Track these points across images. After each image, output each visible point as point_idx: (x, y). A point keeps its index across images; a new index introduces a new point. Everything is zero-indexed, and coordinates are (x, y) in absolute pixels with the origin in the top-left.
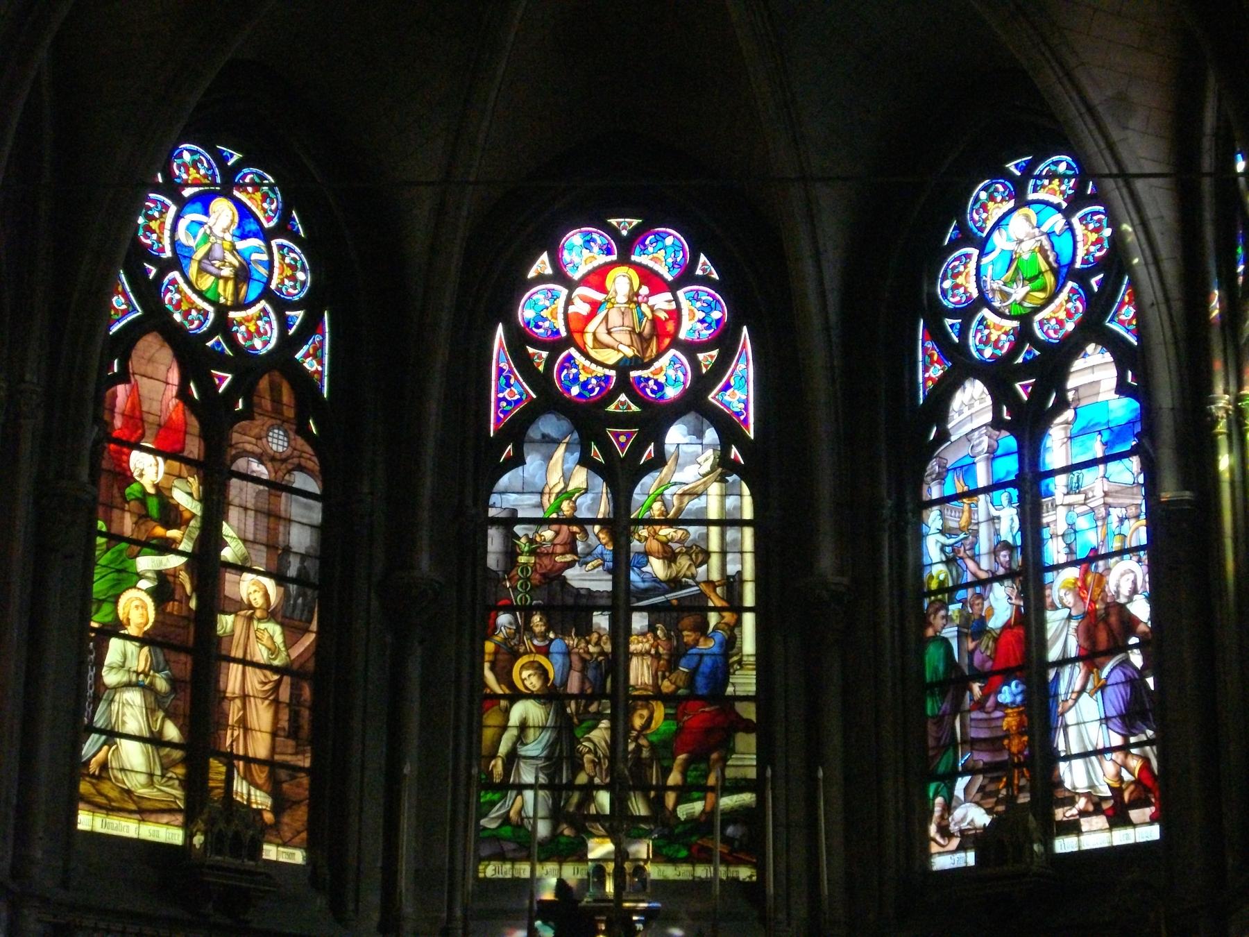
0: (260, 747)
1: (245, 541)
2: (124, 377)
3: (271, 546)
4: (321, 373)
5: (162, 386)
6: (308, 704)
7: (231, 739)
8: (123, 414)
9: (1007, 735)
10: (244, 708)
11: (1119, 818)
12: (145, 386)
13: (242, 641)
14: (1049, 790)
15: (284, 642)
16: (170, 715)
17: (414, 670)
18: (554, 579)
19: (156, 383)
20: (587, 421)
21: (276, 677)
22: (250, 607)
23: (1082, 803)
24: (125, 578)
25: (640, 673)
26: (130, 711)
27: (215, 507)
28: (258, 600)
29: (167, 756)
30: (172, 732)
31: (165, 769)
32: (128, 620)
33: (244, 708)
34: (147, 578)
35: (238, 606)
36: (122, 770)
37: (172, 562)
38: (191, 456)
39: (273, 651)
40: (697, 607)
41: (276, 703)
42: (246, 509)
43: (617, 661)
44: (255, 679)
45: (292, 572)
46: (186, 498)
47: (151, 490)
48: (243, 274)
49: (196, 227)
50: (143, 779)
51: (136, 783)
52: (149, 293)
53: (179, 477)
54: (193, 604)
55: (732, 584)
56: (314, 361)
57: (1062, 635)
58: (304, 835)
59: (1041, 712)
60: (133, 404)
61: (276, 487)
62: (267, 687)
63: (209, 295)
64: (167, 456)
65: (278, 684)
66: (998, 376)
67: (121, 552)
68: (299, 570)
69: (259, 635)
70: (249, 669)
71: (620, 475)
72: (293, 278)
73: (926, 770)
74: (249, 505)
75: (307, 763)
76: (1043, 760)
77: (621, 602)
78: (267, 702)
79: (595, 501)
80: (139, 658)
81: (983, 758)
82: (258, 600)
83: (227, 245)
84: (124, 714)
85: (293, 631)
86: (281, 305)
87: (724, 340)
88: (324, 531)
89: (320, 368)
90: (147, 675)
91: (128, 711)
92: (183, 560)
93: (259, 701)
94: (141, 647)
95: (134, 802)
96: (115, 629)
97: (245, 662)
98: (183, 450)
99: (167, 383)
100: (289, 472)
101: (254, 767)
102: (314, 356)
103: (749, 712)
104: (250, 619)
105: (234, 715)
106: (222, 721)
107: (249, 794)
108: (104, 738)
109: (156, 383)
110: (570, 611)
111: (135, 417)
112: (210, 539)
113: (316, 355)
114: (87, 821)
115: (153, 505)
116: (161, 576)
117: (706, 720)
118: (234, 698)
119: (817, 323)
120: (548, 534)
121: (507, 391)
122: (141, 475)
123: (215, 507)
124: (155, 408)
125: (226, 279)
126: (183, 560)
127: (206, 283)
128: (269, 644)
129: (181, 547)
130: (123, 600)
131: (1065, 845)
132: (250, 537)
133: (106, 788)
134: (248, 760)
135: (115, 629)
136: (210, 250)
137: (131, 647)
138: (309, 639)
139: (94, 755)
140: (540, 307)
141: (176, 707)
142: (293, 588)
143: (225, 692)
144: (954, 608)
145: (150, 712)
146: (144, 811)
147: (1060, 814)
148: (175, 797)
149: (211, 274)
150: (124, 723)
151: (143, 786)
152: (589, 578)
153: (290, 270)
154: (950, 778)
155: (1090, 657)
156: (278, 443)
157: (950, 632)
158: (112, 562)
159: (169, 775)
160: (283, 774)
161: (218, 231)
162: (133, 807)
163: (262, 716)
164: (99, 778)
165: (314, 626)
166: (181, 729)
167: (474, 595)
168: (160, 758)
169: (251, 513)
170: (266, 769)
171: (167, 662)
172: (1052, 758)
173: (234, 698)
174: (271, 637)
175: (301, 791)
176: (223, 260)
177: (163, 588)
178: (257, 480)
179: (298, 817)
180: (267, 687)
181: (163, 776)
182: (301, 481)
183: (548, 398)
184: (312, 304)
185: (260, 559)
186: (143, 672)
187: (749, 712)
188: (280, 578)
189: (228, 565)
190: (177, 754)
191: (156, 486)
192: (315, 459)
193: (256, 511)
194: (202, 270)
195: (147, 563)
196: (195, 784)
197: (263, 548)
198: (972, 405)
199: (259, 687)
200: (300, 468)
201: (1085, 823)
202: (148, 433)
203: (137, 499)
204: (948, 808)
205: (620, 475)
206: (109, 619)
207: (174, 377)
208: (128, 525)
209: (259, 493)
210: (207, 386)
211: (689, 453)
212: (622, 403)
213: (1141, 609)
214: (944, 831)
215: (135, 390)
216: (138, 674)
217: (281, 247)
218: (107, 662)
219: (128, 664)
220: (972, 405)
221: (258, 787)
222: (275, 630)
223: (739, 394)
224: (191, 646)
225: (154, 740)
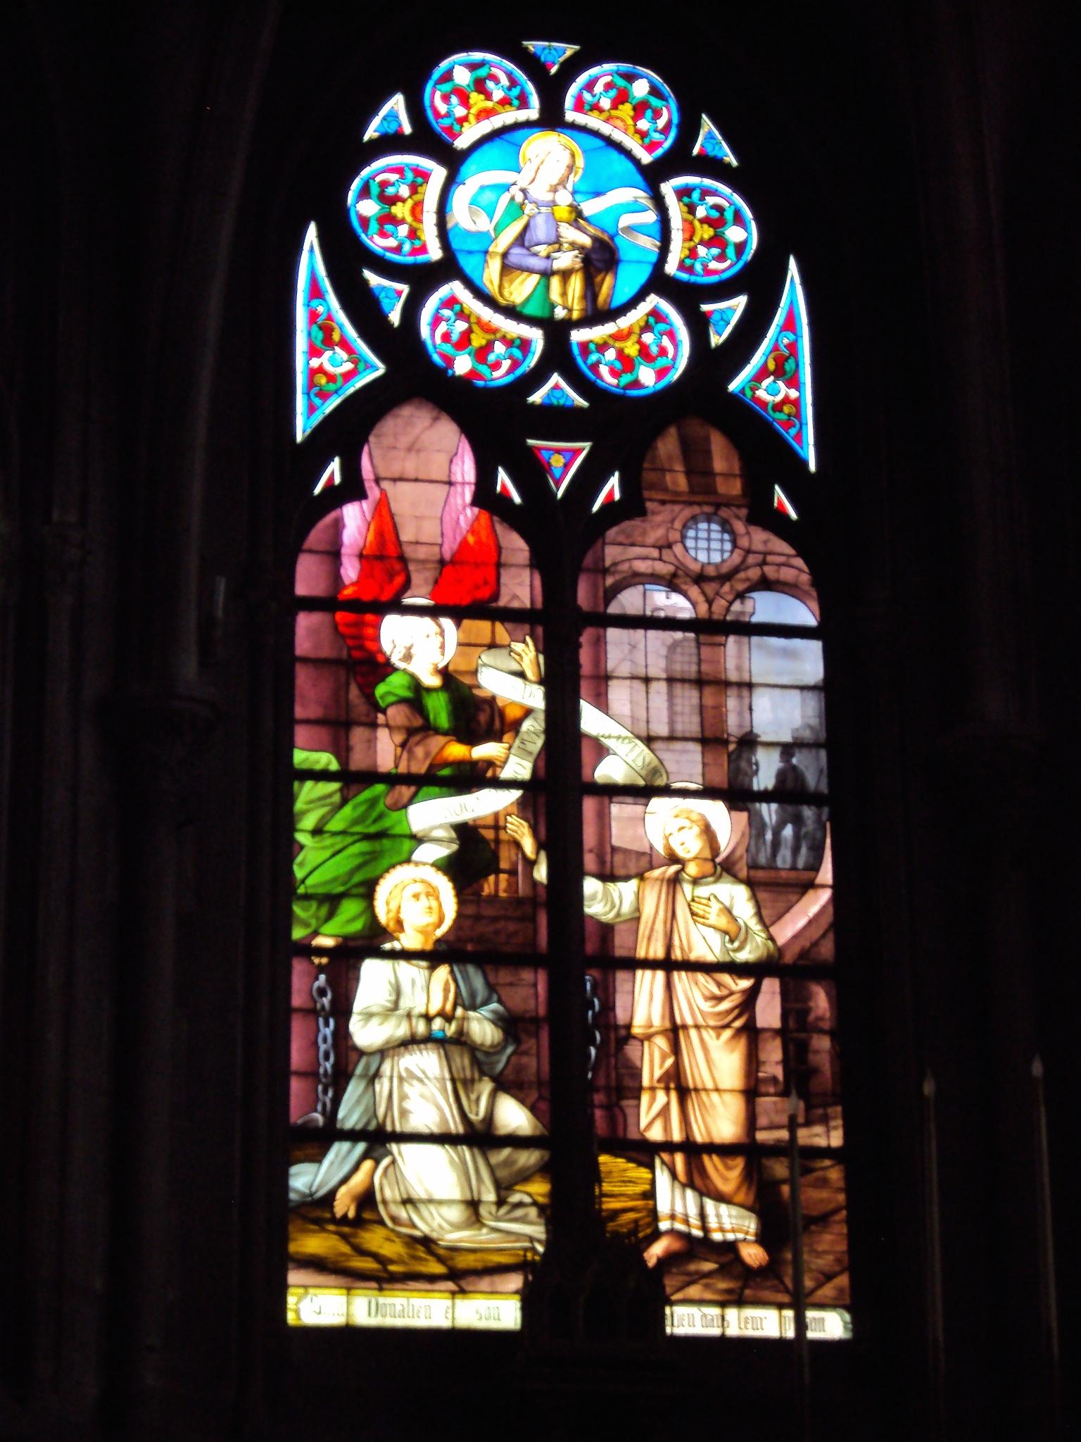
0: (721, 1120)
1: (649, 740)
2: (352, 489)
3: (711, 740)
4: (797, 403)
5: (441, 491)
6: (826, 1025)
7: (653, 1116)
8: (361, 556)
10: (676, 1049)
12: (403, 499)
13: (659, 927)
15: (759, 914)
16: (503, 1085)
21: (745, 984)
22: (673, 859)
24: (382, 845)
26: (421, 1092)
27: (565, 684)
28: (690, 845)
29: (508, 1163)
30: (513, 1116)
31: (503, 1188)
32: (400, 924)
33: (676, 1049)
34: (437, 840)
35: (640, 864)
36: (408, 1201)
37: (481, 805)
38: (516, 604)
39: (734, 934)
41: (751, 1034)
42: (647, 680)
44: (694, 994)
45: (765, 779)
46: (511, 678)
47: (434, 681)
48: (601, 258)
49: (488, 196)
50: (456, 1214)
51: (444, 1224)
53: (492, 645)
54: (541, 873)
56: (783, 381)
58: (843, 1280)
60: (380, 534)
61: (709, 629)
62: (726, 1005)
63: (530, 310)
64: (459, 614)
65: (751, 996)
67: (373, 802)
68: (781, 776)
70: (681, 980)
72: (717, 241)
74: (652, 672)
75: (836, 1139)
78: (728, 1033)
80: (429, 989)
82: (690, 845)
83: (563, 212)
84: (403, 1097)
85: (772, 887)
86: (688, 297)
88: (834, 691)
89: (793, 394)
90: (449, 1018)
91: (412, 1089)
92: (516, 794)
93: (709, 1036)
94: (432, 968)
95: (440, 1260)
96: (372, 941)
97: (668, 965)
98: (496, 596)
99: (450, 483)
100: (741, 596)
101: (712, 1164)
102: (779, 373)
104: (674, 882)
105: (652, 1062)
106: (628, 1082)
107: (703, 1216)
108: (361, 1147)
109: (428, 483)
111: (387, 556)
112: (565, 746)
113: (781, 368)
115: (439, 709)
116: (466, 832)
118: (649, 1037)
122: (408, 657)
123: (565, 684)
124: (430, 531)
125: (566, 275)
126: (516, 794)
127: (520, 290)
128: (723, 922)
129: (505, 774)
130: (383, 891)
132: (661, 729)
133: (374, 1239)
134: (693, 1150)
135: (372, 941)
136: (526, 228)
137: (411, 972)
138: (817, 902)
139: (345, 1180)
141: (520, 1069)
142: (769, 812)
143: (628, 1027)
145: (461, 1085)
146: (460, 1274)
148: (531, 1239)
149: (531, 271)
150: (404, 1113)
151: (457, 1227)
153: (718, 226)
156: (707, 546)
158: (356, 821)
159: (515, 1198)
160: (780, 1169)
161: (540, 192)
162: (438, 1269)
163: (719, 1063)
164: (358, 1223)
165: (826, 874)
166: (533, 1109)
168: (492, 1170)
169: (660, 688)
170: (739, 1163)
171: (491, 988)
173: (649, 1037)
174: (728, 911)
175: (825, 1194)
176: (557, 242)
177: (472, 855)
178: (669, 624)
180: (726, 1005)
181: (500, 1202)
182: (765, 607)
185: (687, 765)
186: (442, 1014)
188: (737, 795)
189: (613, 791)
190: (528, 1158)
191: (445, 673)
192: (799, 562)
193: (671, 680)
194: (507, 269)
195: (435, 816)
197: (695, 748)
199: (707, 1006)
200: (766, 584)
202: (416, 578)
203: (402, 701)
206: (357, 926)
207: (466, 469)
208: (385, 751)
209: (672, 648)
210: (532, 474)
215: (383, 513)
216: (428, 1018)
217: (683, 193)
218: (357, 1007)
219: (405, 1004)
221: (720, 1198)
222: (737, 896)
224: (542, 959)
225: (479, 1137)
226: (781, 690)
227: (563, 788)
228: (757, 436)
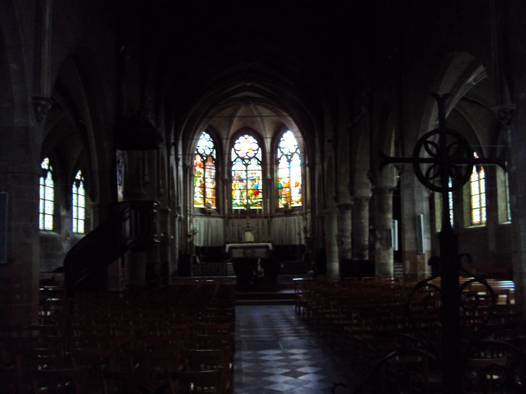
7: (207, 196)
14: (291, 200)
17: (225, 188)
18: (239, 177)
19: (198, 160)
20: (243, 159)
24: (197, 180)
25: (249, 187)
30: (202, 196)
40: (255, 180)
43: (246, 186)
46: (202, 171)
52: (197, 150)
55: (259, 177)
57: (293, 185)
59: (290, 192)
66: (287, 156)
69: (210, 185)
71: (247, 165)
73: (278, 197)
77: (247, 179)
79: (244, 168)
81: (285, 196)
87: (258, 150)
103: (261, 191)
110: (241, 180)
114: (195, 206)
117: (256, 193)
120: (239, 172)
121: (234, 157)
123: (205, 171)
131: (292, 206)
140: (236, 146)
146: (200, 204)
152: (243, 176)
153: (211, 145)
167: (230, 180)
172: (291, 197)
179: (214, 203)
183: (239, 157)
184: (213, 148)
187: (261, 191)
195: (199, 179)
196: (204, 201)
205: (247, 165)
210: (203, 159)
211: (254, 162)
212: (247, 157)
213: (300, 182)
223: (259, 156)
224: (203, 187)
226: (213, 172)
227: (204, 178)
228: (212, 157)
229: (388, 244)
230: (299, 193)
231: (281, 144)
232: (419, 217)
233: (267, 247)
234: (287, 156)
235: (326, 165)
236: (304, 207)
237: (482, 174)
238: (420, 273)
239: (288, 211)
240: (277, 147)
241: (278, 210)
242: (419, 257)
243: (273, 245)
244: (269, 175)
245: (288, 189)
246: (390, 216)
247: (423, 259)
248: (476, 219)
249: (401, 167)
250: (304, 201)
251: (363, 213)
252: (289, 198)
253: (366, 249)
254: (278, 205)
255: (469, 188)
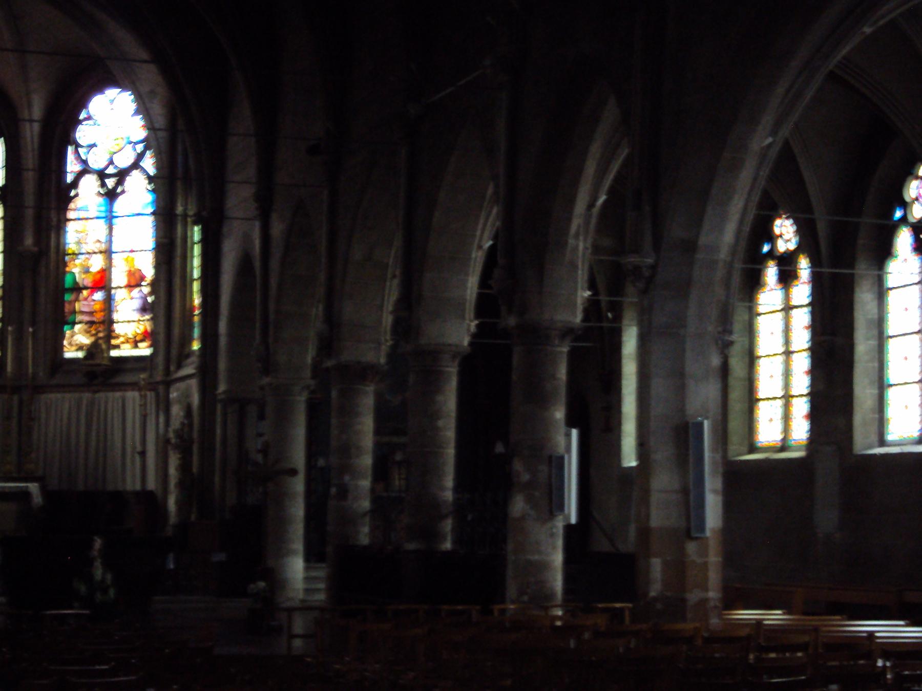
9: (96, 312)
11: (135, 345)
14: (110, 334)
23: (122, 339)
57: (119, 278)
73: (61, 319)
76: (108, 322)
119: (30, 148)
131: (114, 353)
144: (77, 262)
147: (114, 342)
154: (74, 324)
155: (130, 286)
157: (76, 271)
172: (111, 322)
198: (89, 188)
201: (123, 346)
204: (72, 336)
213: (149, 273)
214: (70, 344)
220: (89, 184)
229: (556, 504)
230: (144, 309)
231: (83, 134)
232: (701, 425)
233: (25, 495)
234: (102, 175)
235: (277, 229)
236: (160, 359)
237: (802, 292)
238: (693, 597)
239: (102, 370)
240: (67, 139)
241: (59, 364)
242: (691, 548)
243: (44, 490)
244: (29, 241)
245: (99, 296)
246: (559, 414)
247: (704, 552)
248: (768, 432)
249: (647, 273)
250: (161, 337)
251: (440, 398)
252: (104, 324)
253: (446, 516)
254: (59, 348)
255: (750, 332)
